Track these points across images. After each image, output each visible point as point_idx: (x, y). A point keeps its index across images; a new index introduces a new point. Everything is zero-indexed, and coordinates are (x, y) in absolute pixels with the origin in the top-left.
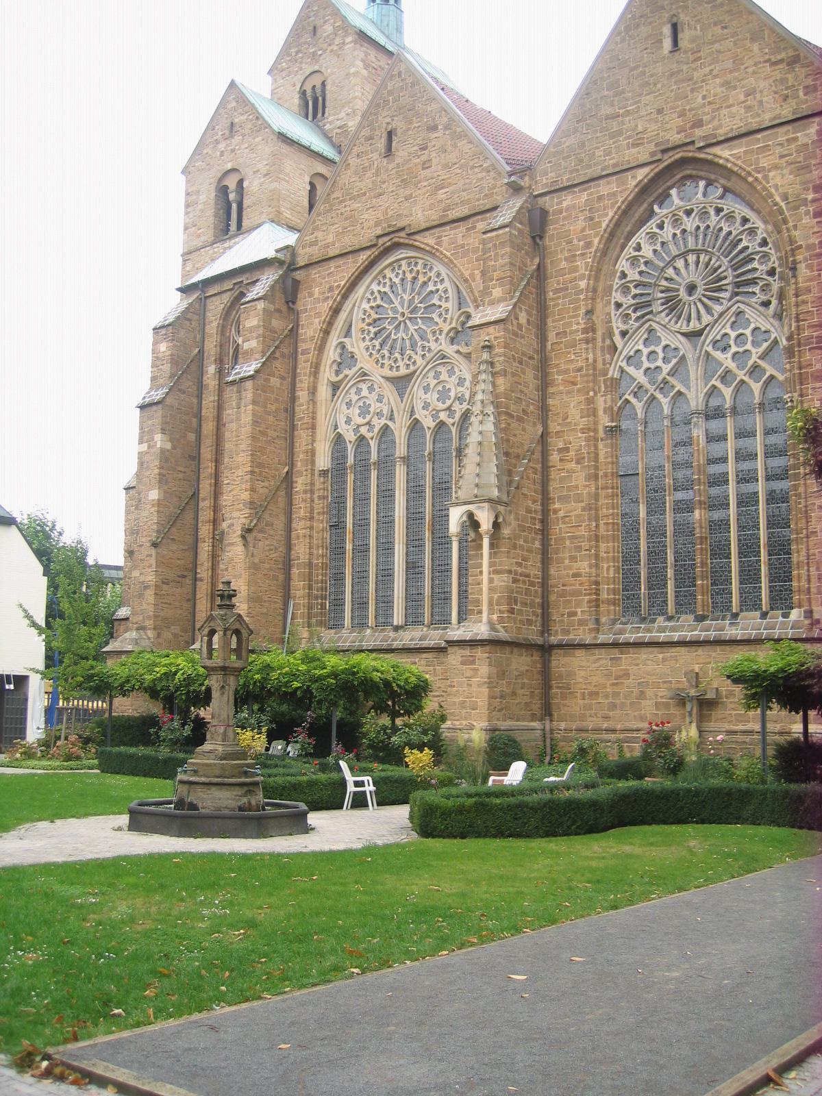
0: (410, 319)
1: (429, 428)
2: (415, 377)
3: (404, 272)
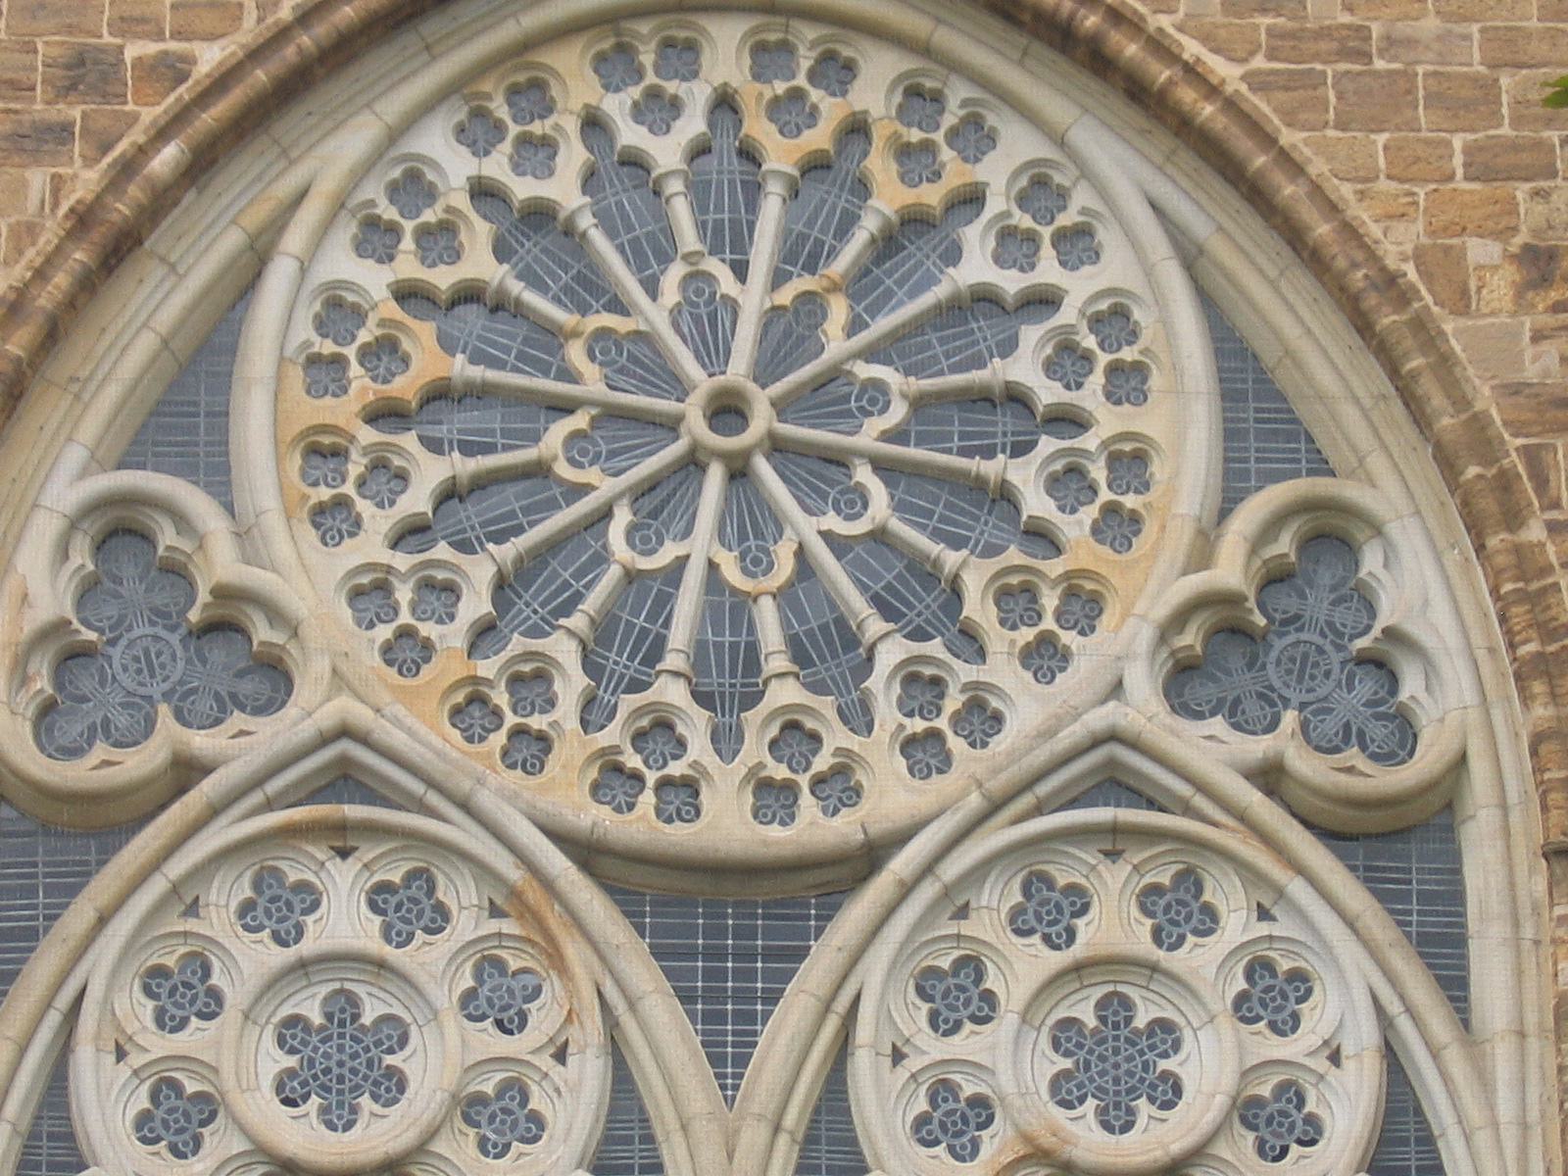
0: (777, 448)
2: (880, 887)
3: (725, 103)
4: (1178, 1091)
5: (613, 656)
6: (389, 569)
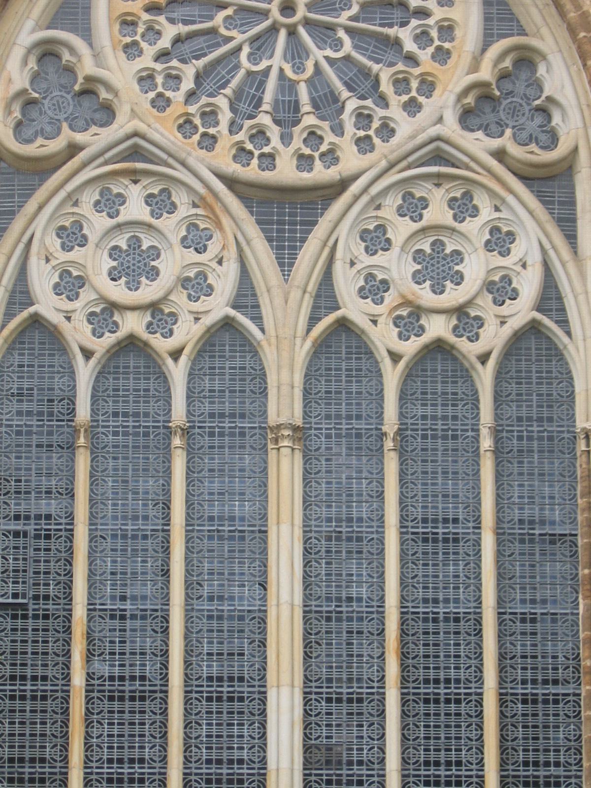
1: (395, 357)
4: (462, 278)
5: (242, 105)
6: (154, 70)
